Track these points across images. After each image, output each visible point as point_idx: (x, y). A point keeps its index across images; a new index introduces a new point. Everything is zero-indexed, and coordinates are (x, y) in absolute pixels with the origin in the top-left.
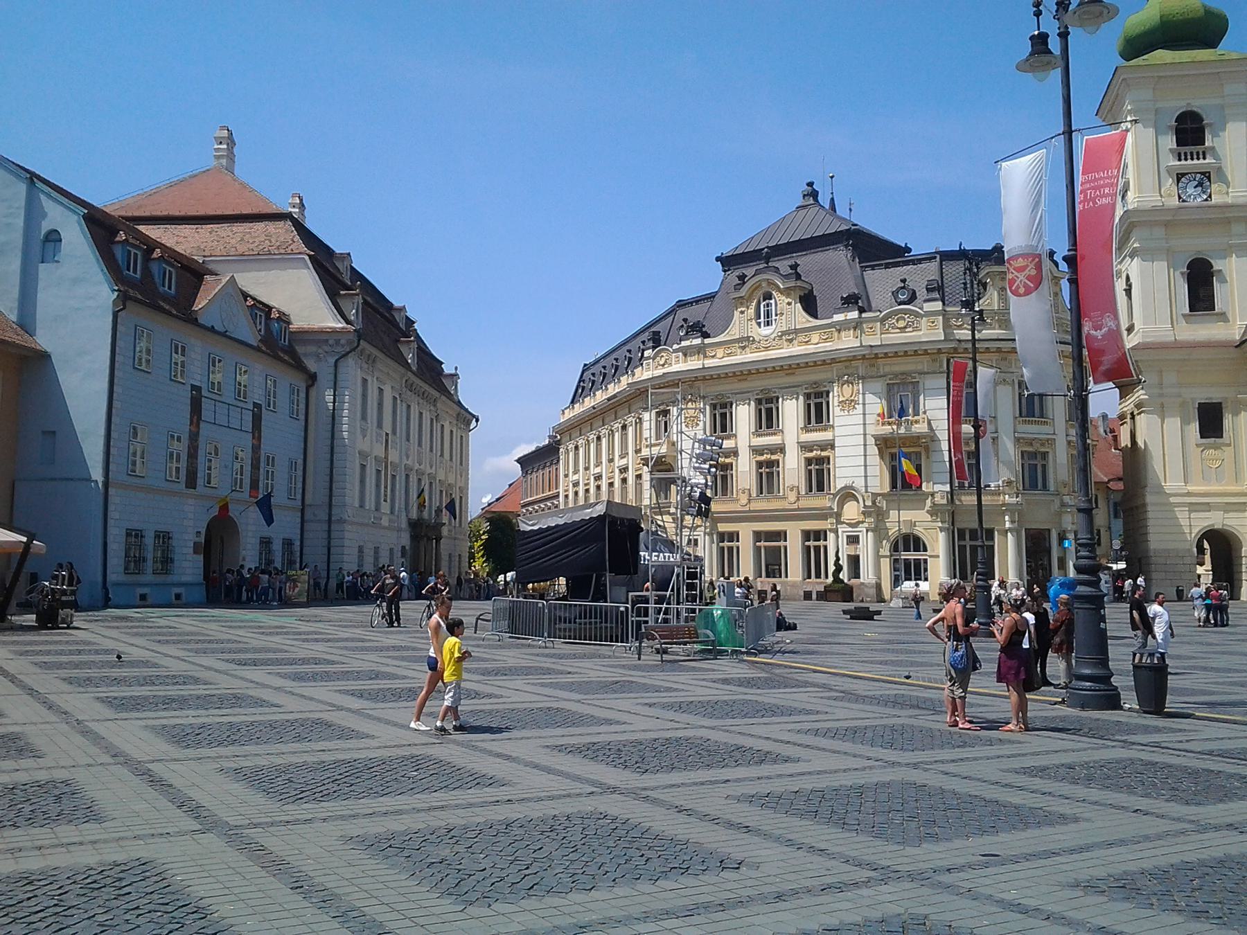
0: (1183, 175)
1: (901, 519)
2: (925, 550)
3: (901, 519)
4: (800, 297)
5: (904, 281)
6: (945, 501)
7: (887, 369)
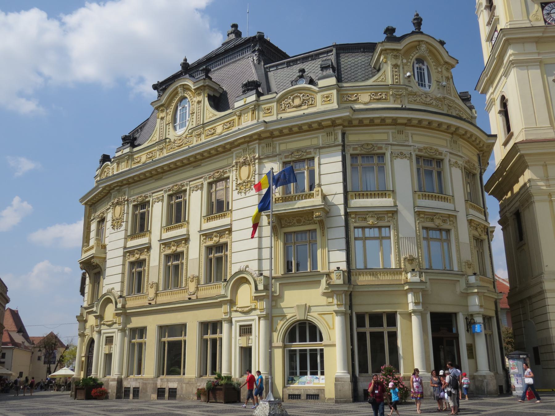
0: (546, 4)
1: (298, 301)
2: (321, 339)
3: (298, 301)
4: (210, 98)
5: (303, 71)
6: (340, 282)
7: (283, 147)
